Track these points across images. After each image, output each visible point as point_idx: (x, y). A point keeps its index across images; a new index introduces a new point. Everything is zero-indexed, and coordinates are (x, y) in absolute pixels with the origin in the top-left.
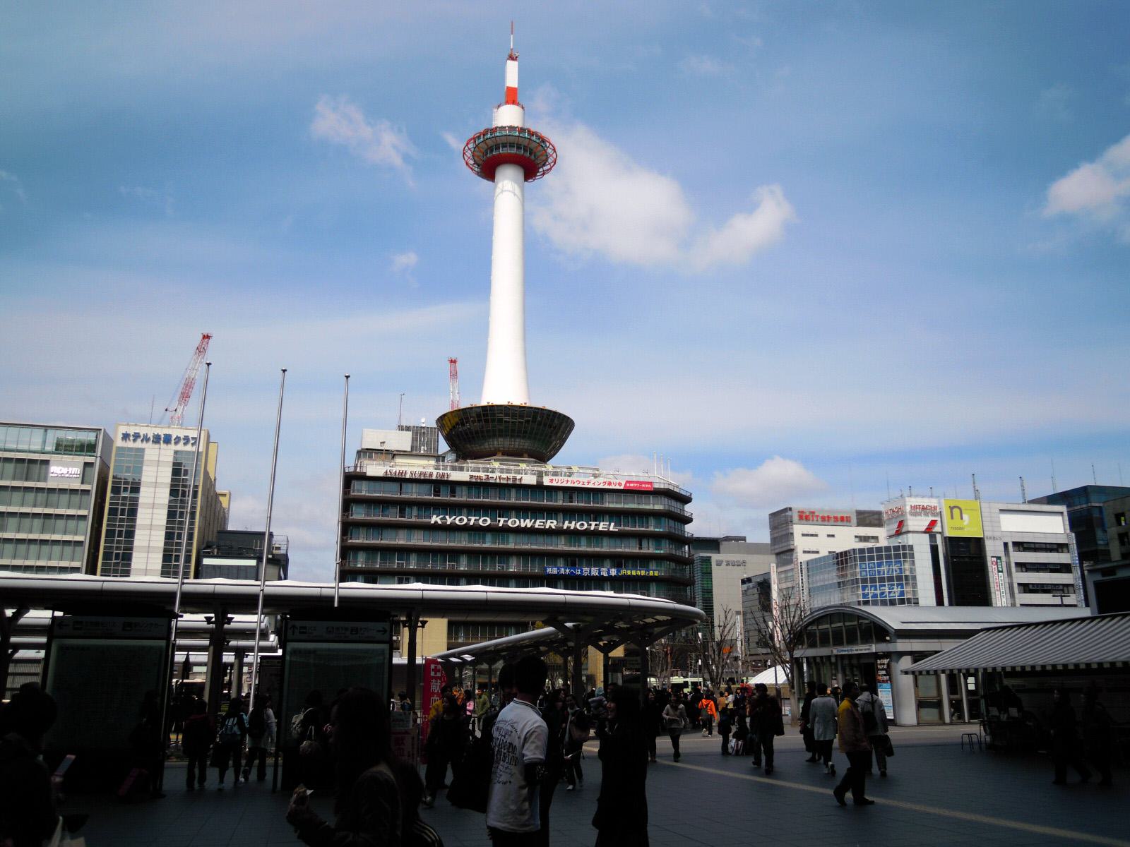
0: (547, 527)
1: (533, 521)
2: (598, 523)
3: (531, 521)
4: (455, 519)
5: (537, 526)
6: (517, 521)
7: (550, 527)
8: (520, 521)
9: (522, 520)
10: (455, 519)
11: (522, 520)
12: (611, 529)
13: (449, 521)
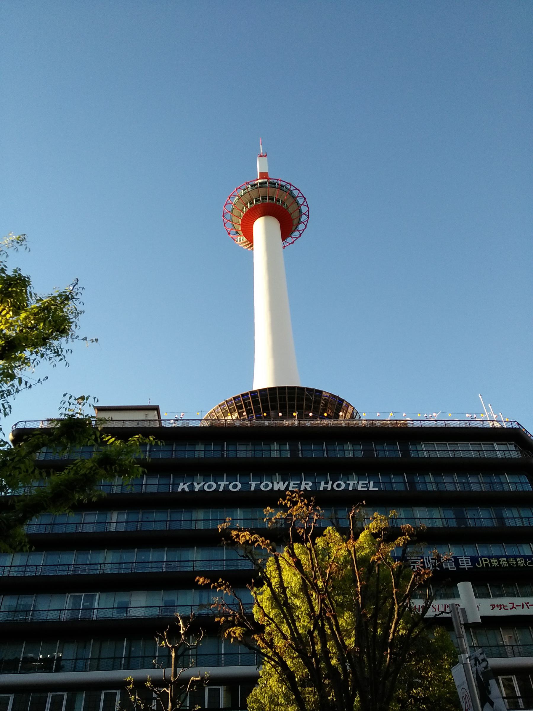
1: (287, 483)
3: (284, 484)
4: (204, 485)
6: (269, 483)
8: (272, 483)
9: (275, 483)
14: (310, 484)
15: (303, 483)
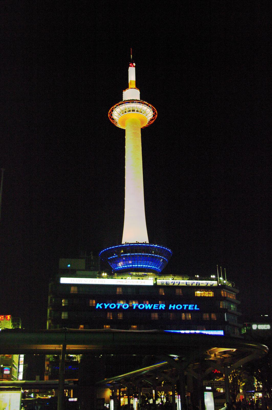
0: (160, 308)
1: (152, 305)
2: (188, 305)
3: (151, 305)
4: (109, 306)
5: (154, 308)
7: (162, 308)
9: (146, 305)
10: (109, 306)
11: (146, 305)
12: (195, 308)
13: (106, 306)
14: (164, 306)
15: (161, 305)
